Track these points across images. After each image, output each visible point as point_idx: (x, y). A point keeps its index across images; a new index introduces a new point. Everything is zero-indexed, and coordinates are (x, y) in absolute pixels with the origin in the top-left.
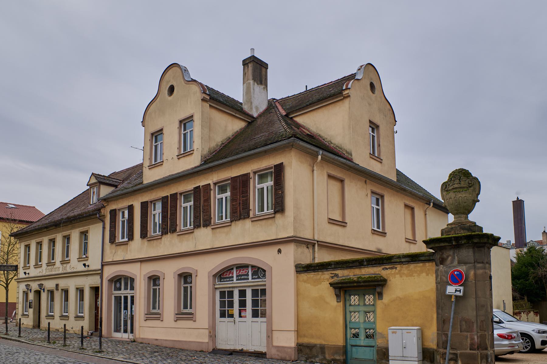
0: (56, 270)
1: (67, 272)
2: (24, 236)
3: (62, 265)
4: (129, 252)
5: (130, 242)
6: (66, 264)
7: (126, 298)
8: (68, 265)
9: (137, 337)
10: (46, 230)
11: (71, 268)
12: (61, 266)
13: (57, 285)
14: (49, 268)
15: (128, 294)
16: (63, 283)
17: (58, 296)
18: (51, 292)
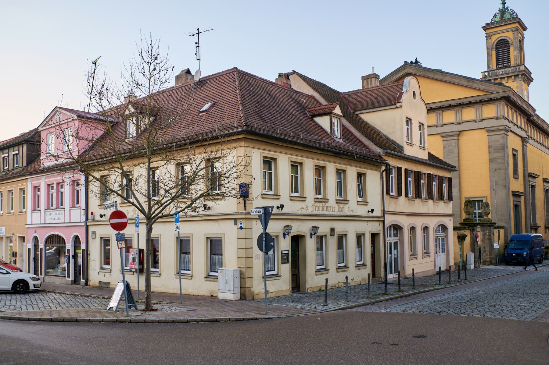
0: (330, 210)
1: (345, 214)
6: (343, 205)
8: (346, 207)
10: (319, 152)
11: (350, 211)
12: (336, 205)
13: (332, 230)
14: (319, 205)
16: (340, 227)
17: (332, 243)
18: (321, 239)
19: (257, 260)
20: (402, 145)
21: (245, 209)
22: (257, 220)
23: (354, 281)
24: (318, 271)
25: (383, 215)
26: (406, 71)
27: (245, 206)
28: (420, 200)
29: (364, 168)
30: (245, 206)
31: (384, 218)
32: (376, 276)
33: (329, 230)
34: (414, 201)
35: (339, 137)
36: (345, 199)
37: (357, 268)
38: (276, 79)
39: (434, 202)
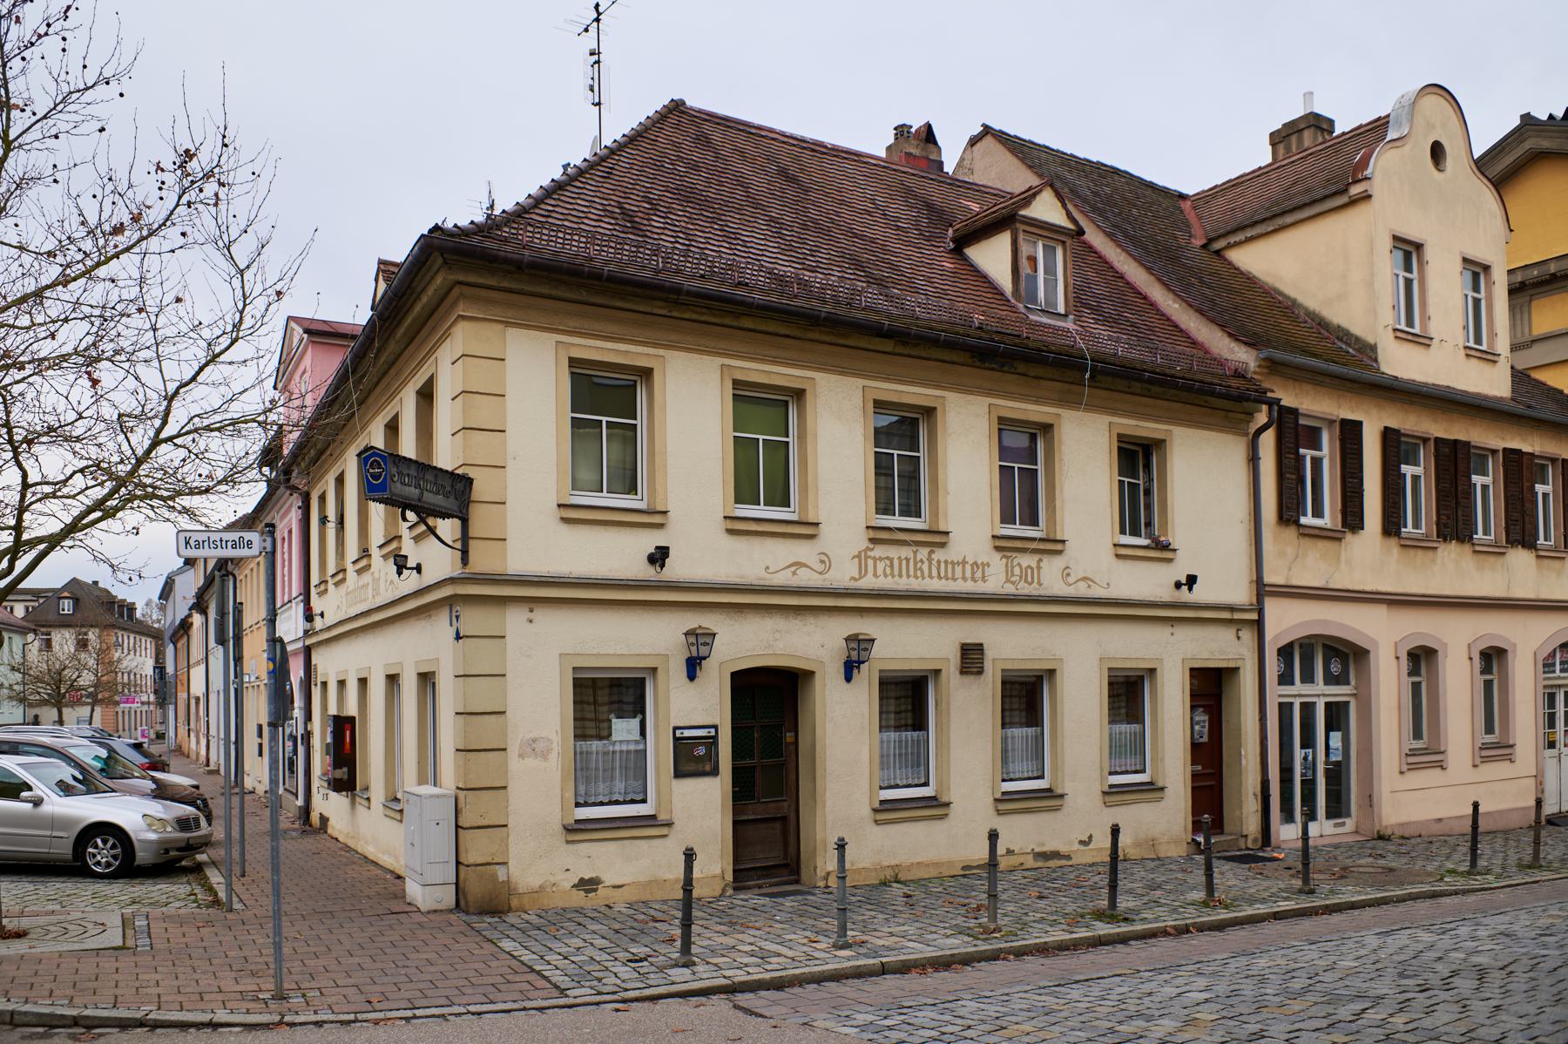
1: (1042, 592)
2: (620, 304)
3: (1007, 557)
4: (1343, 566)
5: (1349, 537)
6: (1036, 557)
7: (1308, 709)
9: (1384, 823)
10: (889, 349)
11: (1071, 580)
15: (1319, 696)
19: (531, 762)
20: (1372, 341)
21: (465, 560)
22: (532, 605)
23: (1091, 846)
24: (886, 806)
25: (1255, 602)
26: (1527, 145)
27: (465, 553)
28: (1467, 548)
29: (1158, 419)
30: (465, 553)
31: (1261, 612)
32: (1226, 831)
33: (954, 656)
34: (1430, 553)
35: (1061, 309)
36: (1051, 537)
37: (1108, 799)
38: (889, 149)
39: (1538, 557)
